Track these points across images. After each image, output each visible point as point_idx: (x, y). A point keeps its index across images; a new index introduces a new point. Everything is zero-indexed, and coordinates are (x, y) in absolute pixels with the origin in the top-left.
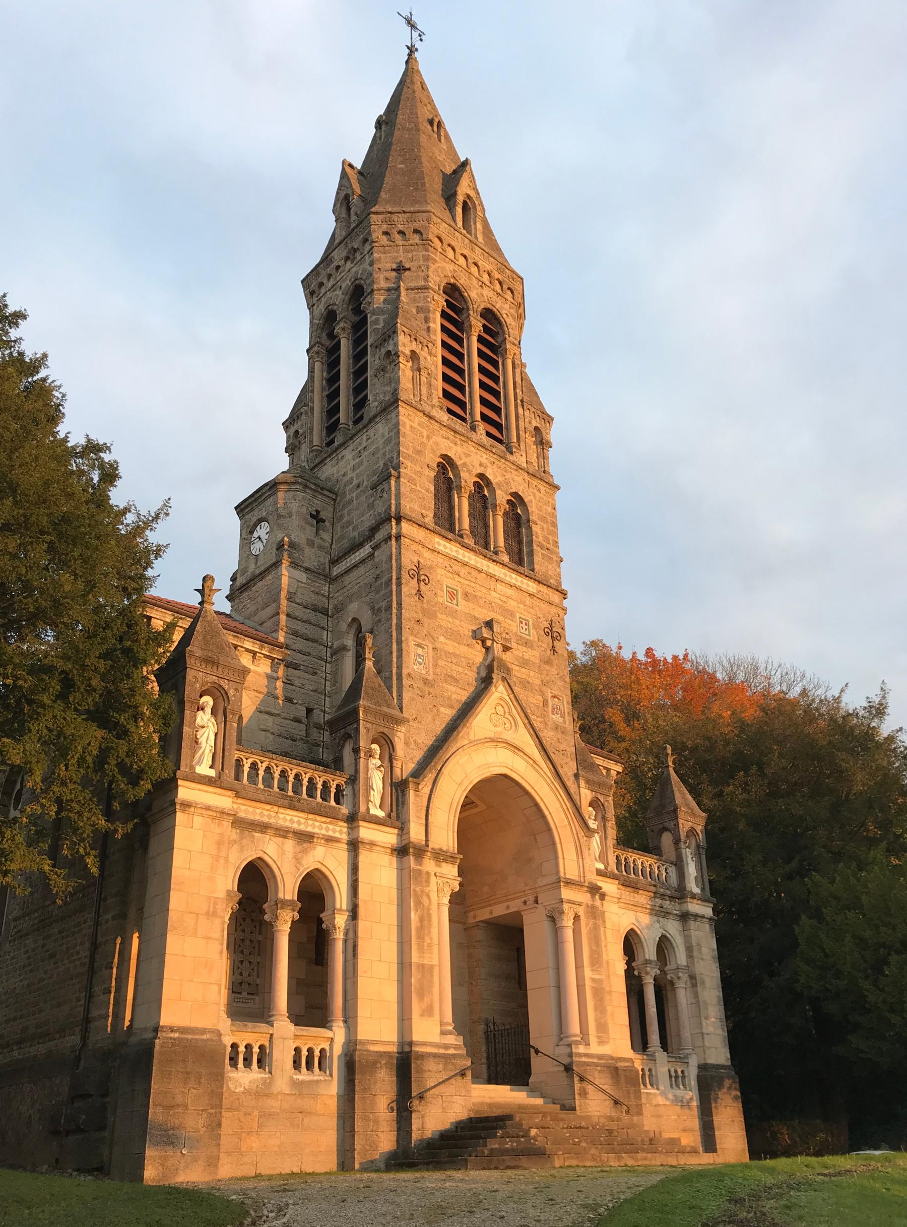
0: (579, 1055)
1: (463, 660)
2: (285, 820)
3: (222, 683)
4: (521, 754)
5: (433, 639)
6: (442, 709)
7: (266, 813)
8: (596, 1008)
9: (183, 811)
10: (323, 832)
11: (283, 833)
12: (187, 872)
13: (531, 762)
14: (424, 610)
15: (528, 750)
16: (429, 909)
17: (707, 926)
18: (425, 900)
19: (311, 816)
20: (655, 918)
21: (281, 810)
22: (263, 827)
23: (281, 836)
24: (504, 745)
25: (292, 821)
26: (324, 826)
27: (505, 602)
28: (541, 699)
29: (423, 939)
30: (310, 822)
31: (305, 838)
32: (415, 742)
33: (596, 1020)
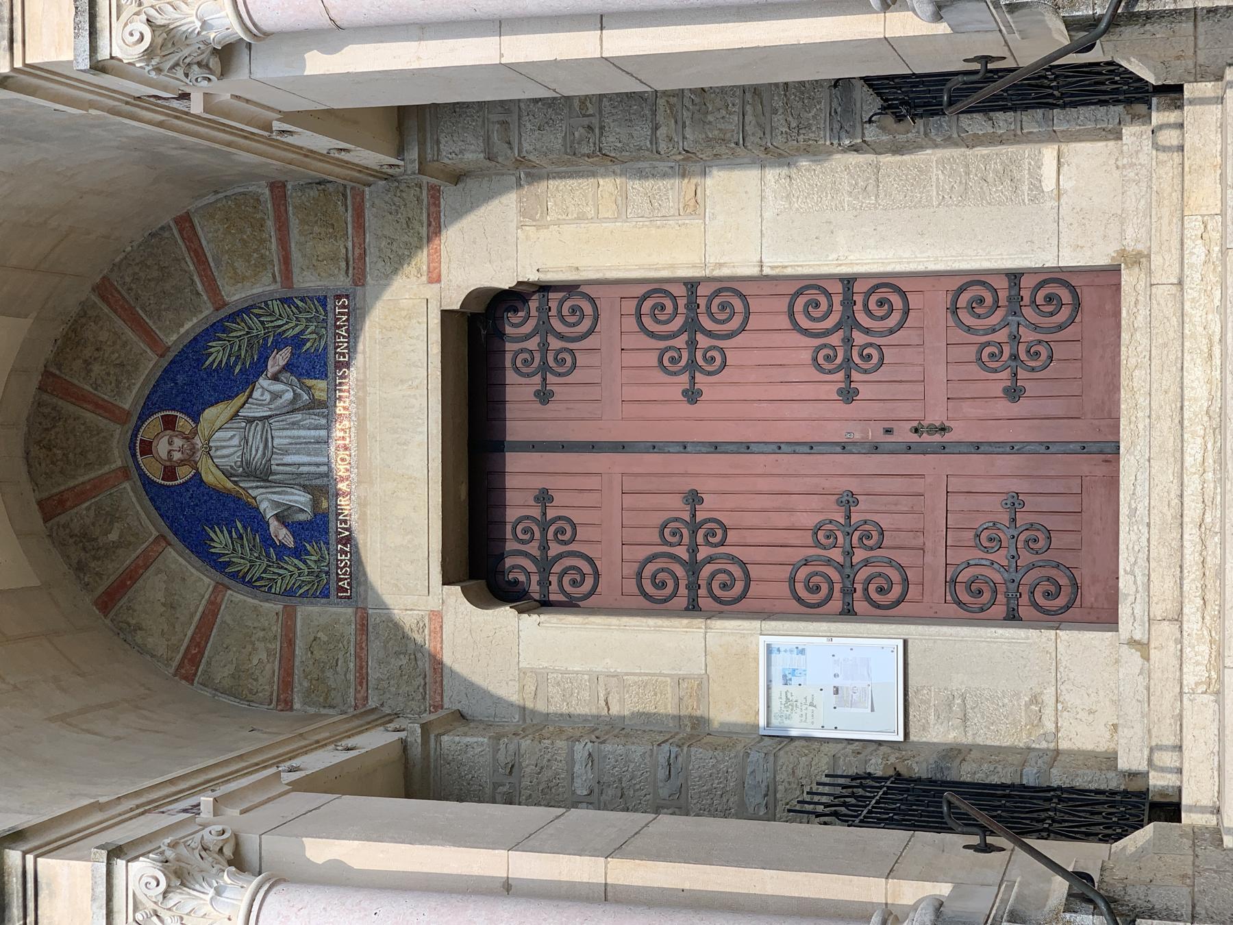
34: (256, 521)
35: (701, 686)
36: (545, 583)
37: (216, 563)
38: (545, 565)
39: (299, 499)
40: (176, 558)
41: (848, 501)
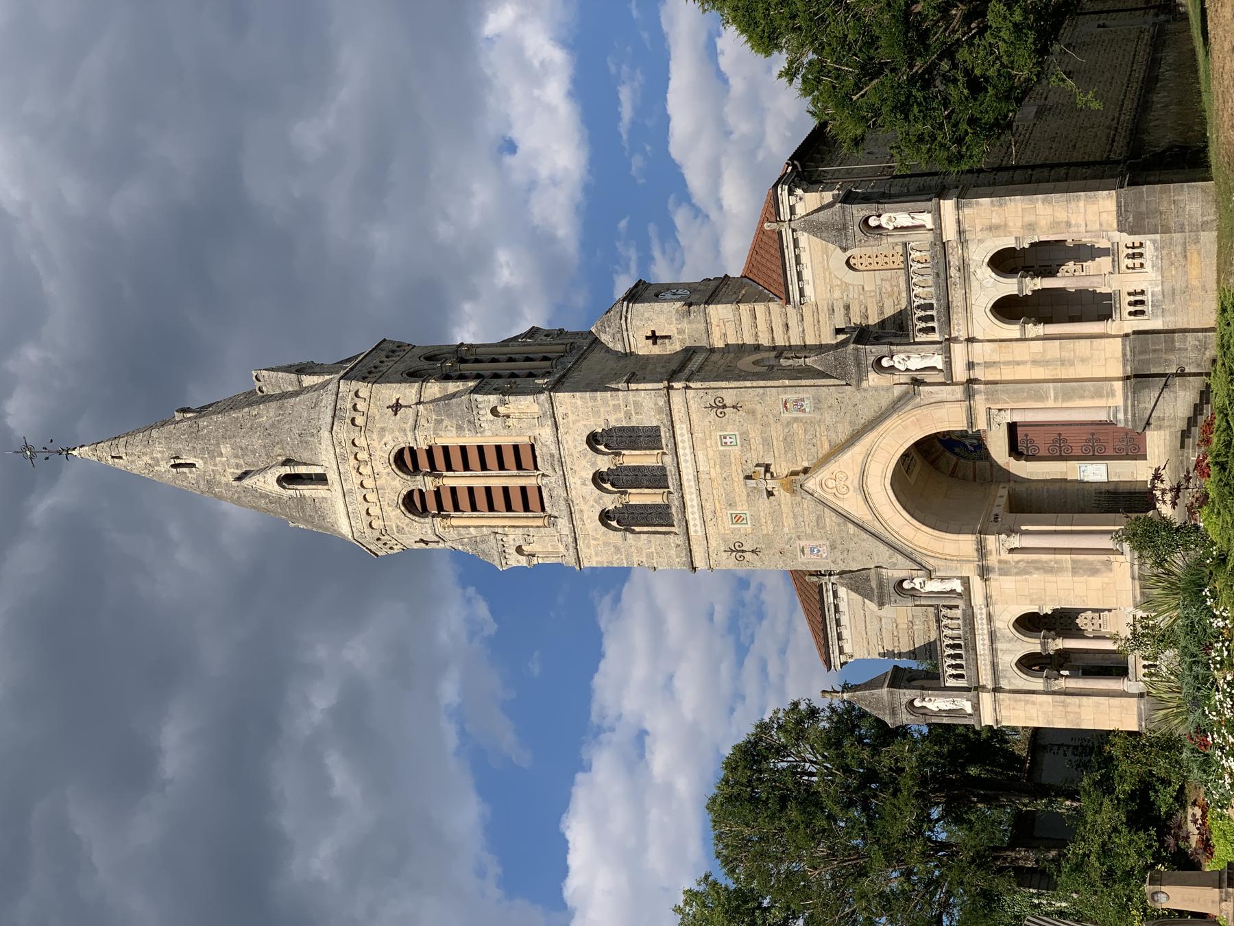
0: (1126, 420)
1: (796, 510)
2: (984, 649)
3: (904, 703)
4: (866, 469)
5: (791, 539)
6: (851, 531)
7: (983, 662)
8: (1082, 397)
9: (1001, 722)
10: (985, 627)
11: (994, 651)
12: (1040, 718)
13: (870, 457)
14: (769, 547)
15: (860, 459)
16: (1028, 562)
17: (967, 211)
18: (1022, 565)
19: (976, 633)
20: (972, 277)
21: (978, 653)
22: (994, 666)
23: (996, 651)
24: (864, 486)
25: (984, 645)
26: (980, 622)
27: (715, 462)
28: (795, 425)
29: (1052, 567)
30: (980, 632)
31: (993, 636)
32: (890, 558)
33: (1092, 397)
34: (965, 446)
35: (1066, 473)
36: (1028, 451)
37: (956, 454)
38: (1027, 448)
39: (975, 441)
40: (948, 454)
41: (1093, 434)
